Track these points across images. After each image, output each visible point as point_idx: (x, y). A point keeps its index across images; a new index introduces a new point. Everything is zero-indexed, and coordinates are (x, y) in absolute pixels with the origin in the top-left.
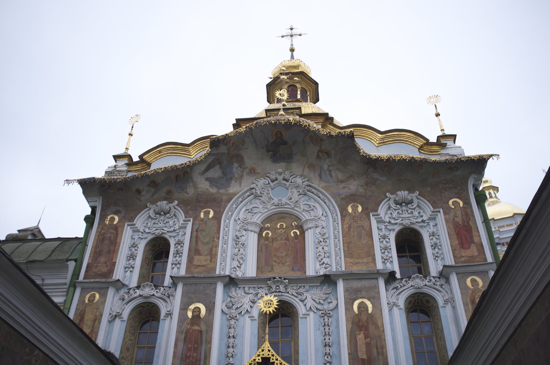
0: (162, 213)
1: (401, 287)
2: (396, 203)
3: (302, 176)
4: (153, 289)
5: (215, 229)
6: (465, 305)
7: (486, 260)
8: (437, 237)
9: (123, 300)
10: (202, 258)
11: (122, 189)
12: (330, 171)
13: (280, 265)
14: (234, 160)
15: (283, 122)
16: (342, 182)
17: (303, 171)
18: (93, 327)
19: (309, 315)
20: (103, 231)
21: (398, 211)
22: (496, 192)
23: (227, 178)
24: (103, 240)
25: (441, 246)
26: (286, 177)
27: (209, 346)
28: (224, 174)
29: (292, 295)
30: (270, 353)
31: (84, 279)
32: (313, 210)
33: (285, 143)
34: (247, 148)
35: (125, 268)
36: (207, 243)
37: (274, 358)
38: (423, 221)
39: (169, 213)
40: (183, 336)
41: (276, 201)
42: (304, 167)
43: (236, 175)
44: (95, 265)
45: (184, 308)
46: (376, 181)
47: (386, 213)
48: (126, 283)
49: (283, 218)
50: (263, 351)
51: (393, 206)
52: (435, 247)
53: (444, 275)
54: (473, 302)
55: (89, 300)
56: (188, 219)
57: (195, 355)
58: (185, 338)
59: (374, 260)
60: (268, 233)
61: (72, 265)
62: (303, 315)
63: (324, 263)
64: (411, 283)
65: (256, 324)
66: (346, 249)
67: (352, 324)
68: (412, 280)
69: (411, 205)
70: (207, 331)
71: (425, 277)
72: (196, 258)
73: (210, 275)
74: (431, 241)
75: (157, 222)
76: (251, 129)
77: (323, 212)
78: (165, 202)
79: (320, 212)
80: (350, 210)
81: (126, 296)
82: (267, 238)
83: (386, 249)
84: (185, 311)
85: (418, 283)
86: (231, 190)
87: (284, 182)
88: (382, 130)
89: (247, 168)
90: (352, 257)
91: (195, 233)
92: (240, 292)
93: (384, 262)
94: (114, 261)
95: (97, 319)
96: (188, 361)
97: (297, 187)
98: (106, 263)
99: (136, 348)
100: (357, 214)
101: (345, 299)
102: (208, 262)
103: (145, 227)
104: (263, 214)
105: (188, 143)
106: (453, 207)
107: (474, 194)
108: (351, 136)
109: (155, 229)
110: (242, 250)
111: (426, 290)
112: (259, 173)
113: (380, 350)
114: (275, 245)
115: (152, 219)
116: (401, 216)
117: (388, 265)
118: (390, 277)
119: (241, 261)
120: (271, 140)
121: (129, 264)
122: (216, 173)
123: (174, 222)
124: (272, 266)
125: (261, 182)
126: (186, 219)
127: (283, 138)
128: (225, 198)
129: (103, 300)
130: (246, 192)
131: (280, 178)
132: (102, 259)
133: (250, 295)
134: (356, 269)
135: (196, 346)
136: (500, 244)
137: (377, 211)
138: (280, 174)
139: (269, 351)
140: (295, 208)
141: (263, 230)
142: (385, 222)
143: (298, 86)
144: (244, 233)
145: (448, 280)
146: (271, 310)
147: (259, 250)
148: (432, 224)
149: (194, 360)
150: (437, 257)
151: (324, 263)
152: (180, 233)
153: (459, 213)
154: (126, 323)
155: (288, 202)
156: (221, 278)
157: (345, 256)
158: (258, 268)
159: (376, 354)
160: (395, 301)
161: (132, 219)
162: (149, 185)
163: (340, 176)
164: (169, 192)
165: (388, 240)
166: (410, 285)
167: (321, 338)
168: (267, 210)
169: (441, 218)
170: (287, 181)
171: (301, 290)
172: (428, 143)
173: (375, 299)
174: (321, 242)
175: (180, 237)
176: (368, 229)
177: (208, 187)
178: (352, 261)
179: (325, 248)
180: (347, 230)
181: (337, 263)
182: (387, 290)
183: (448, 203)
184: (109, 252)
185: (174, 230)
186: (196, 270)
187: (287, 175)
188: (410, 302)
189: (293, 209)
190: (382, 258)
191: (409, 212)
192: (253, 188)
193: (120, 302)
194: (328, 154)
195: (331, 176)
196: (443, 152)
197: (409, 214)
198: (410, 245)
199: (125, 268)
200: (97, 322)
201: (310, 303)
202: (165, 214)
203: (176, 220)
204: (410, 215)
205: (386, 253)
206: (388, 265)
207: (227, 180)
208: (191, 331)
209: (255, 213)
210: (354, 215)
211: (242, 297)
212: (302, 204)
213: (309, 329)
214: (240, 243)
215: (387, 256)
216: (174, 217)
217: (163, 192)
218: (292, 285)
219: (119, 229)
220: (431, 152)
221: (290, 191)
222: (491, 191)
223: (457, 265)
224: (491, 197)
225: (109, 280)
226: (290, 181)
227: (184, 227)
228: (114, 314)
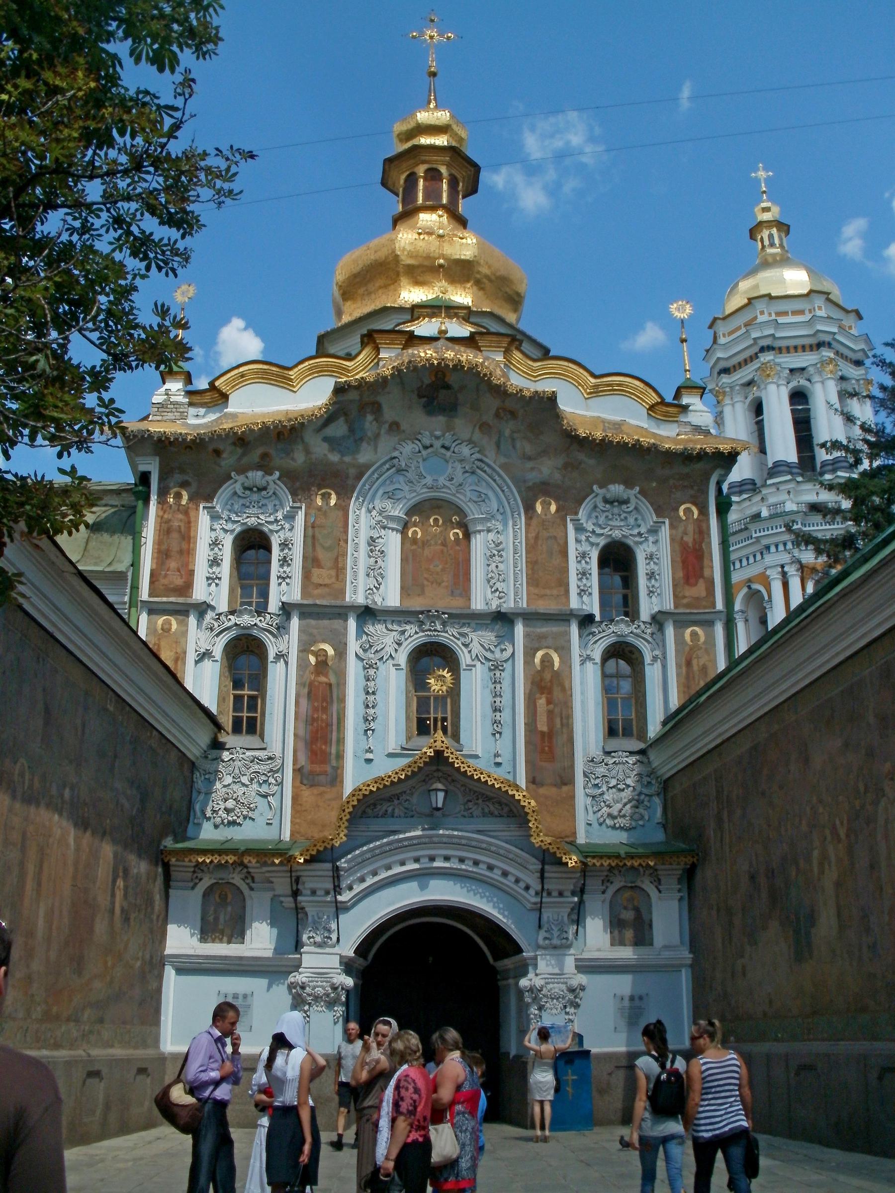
0: (255, 489)
1: (600, 632)
3: (470, 441)
4: (253, 616)
5: (340, 525)
6: (678, 666)
7: (714, 607)
8: (656, 560)
9: (212, 629)
10: (323, 572)
11: (190, 447)
12: (513, 440)
13: (434, 585)
14: (368, 410)
15: (451, 364)
16: (530, 458)
17: (473, 433)
18: (176, 668)
19: (474, 666)
20: (166, 516)
21: (607, 514)
22: (783, 235)
23: (356, 438)
24: (168, 531)
25: (659, 575)
26: (447, 444)
27: (342, 705)
28: (352, 430)
29: (453, 635)
30: (444, 745)
31: (150, 595)
32: (484, 501)
33: (448, 387)
34: (389, 393)
35: (208, 579)
36: (329, 549)
37: (449, 751)
38: (640, 534)
39: (265, 489)
40: (306, 690)
41: (429, 480)
42: (475, 426)
43: (369, 434)
44: (163, 573)
45: (304, 650)
46: (580, 463)
47: (589, 517)
48: (212, 603)
49: (439, 507)
50: (435, 741)
51: (601, 505)
52: (651, 578)
53: (658, 620)
54: (689, 663)
55: (162, 629)
56: (298, 505)
57: (324, 717)
58: (309, 693)
59: (567, 592)
60: (415, 532)
61: (130, 574)
62: (467, 666)
63: (497, 590)
64: (613, 628)
65: (403, 675)
66: (530, 572)
67: (532, 683)
68: (615, 625)
69: (624, 507)
70: (338, 684)
71: (633, 621)
72: (316, 572)
73: (338, 603)
74: (648, 567)
75: (248, 504)
76: (400, 371)
77: (498, 506)
78: (260, 473)
79: (495, 505)
80: (539, 508)
81: (216, 625)
82: (414, 541)
83: (584, 574)
84: (305, 653)
85: (622, 629)
86: (363, 457)
87: (443, 451)
88: (597, 373)
89: (386, 422)
90: (537, 586)
91: (310, 529)
92: (380, 627)
93: (579, 594)
94: (190, 567)
95: (180, 657)
96: (315, 724)
97: (461, 461)
98: (179, 571)
99: (232, 697)
100: (549, 517)
101: (525, 647)
102: (333, 580)
103: (230, 511)
104: (409, 500)
105: (290, 365)
106: (684, 518)
107: (717, 498)
108: (552, 399)
109: (245, 516)
110: (380, 562)
111: (631, 639)
112: (404, 431)
113: (565, 721)
114: (427, 552)
115: (239, 496)
116: (611, 523)
117: (585, 598)
118: (587, 620)
119: (380, 579)
120: (427, 381)
121: (214, 573)
122: (339, 429)
123: (275, 505)
124: (423, 587)
125: (408, 448)
126: (295, 505)
127: (446, 379)
128: (352, 471)
129: (184, 629)
130: (384, 463)
131: (438, 444)
132: (173, 564)
133: (394, 633)
134: (542, 606)
135: (325, 704)
136: (773, 349)
137: (576, 513)
138: (437, 438)
139: (443, 742)
140: (458, 495)
141: (409, 525)
142: (586, 531)
143: (443, 170)
144: (383, 532)
145: (661, 628)
146: (444, 688)
147: (404, 560)
148: (651, 539)
149: (324, 725)
150: (651, 592)
151: (497, 590)
152: (287, 526)
153: (691, 528)
154: (219, 663)
155: (448, 484)
156: (353, 608)
157: (527, 583)
158: (402, 588)
159: (558, 725)
160: (588, 652)
161: (209, 498)
162: (234, 444)
163: (528, 449)
164: (265, 456)
165: (588, 560)
166: (611, 631)
167: (490, 699)
168: (415, 494)
169: (665, 532)
170: (447, 449)
171: (465, 630)
172: (663, 403)
173: (564, 650)
174: (494, 555)
175: (288, 534)
176: (562, 542)
177: (326, 452)
178: (536, 591)
179: (499, 565)
180: (532, 541)
181: (515, 596)
182: (580, 636)
183: (677, 510)
184: (181, 552)
185: (276, 520)
186: (316, 592)
187: (448, 439)
188: (609, 652)
189: (454, 495)
190: (579, 587)
191: (622, 517)
192: (395, 458)
193: (208, 633)
194: (513, 414)
195: (514, 447)
196: (682, 418)
197: (622, 520)
198: (617, 560)
199: (208, 579)
200: (179, 662)
201: (476, 648)
202: (261, 489)
203: (277, 503)
204: (622, 524)
205: (584, 581)
206: (585, 598)
207: (355, 441)
208: (316, 683)
209: (398, 499)
210: (543, 517)
211: (384, 635)
212: (467, 490)
213: (475, 685)
214: (377, 549)
215: (585, 585)
216: (273, 497)
217: (255, 455)
218: (452, 621)
219: (192, 514)
220: (665, 416)
221: (450, 465)
222: (774, 231)
223: (676, 611)
224: (772, 245)
225: (189, 601)
226: (452, 449)
227: (290, 517)
228: (203, 650)
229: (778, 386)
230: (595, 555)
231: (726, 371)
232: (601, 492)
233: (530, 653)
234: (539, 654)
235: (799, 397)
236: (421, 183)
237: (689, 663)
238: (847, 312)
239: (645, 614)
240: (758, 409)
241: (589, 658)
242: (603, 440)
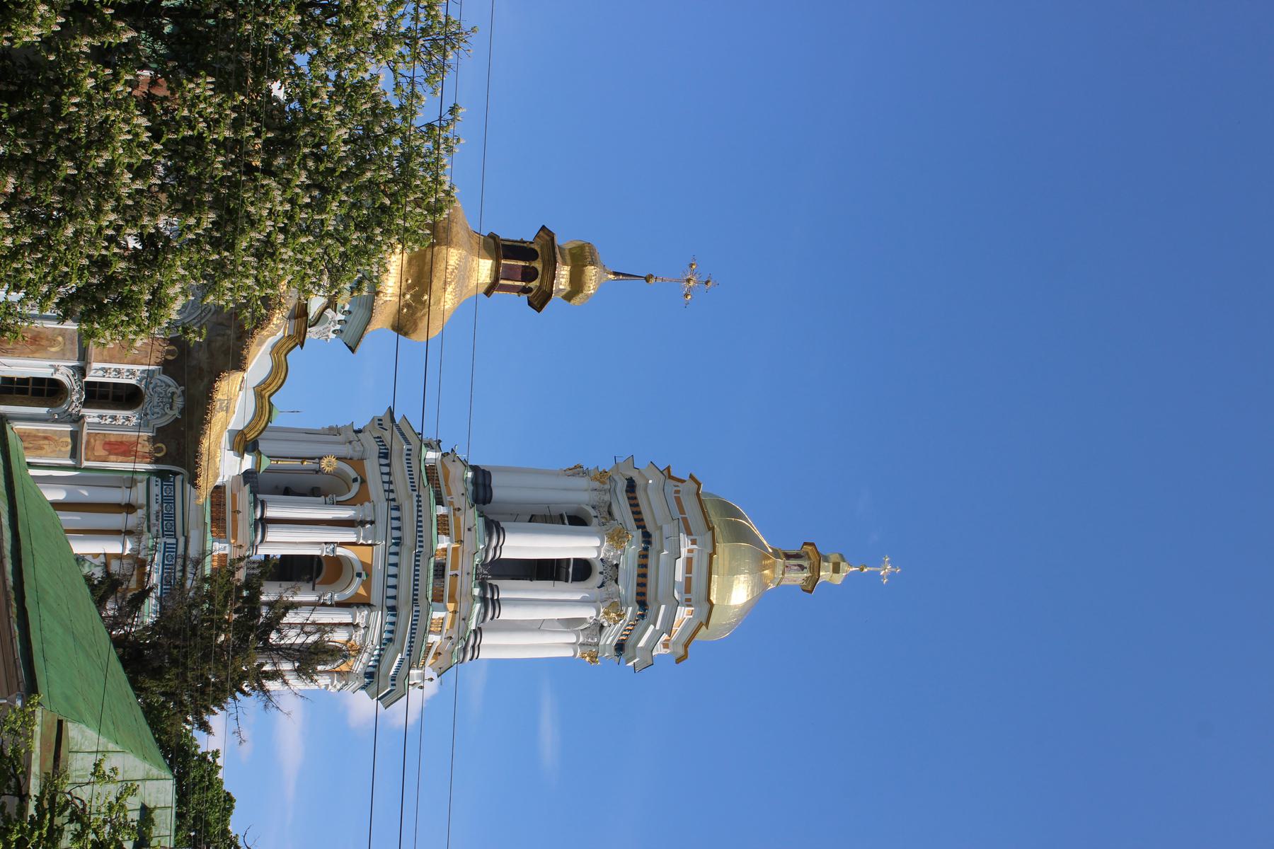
2: (173, 393)
54: (46, 438)
83: (119, 372)
85: (76, 397)
118: (82, 371)
229: (599, 548)
230: (133, 382)
231: (631, 486)
232: (179, 392)
233: (63, 333)
234: (60, 339)
235: (582, 570)
236: (522, 263)
237: (46, 438)
238: (686, 646)
239: (85, 411)
240: (577, 520)
241: (57, 370)
242: (211, 398)
